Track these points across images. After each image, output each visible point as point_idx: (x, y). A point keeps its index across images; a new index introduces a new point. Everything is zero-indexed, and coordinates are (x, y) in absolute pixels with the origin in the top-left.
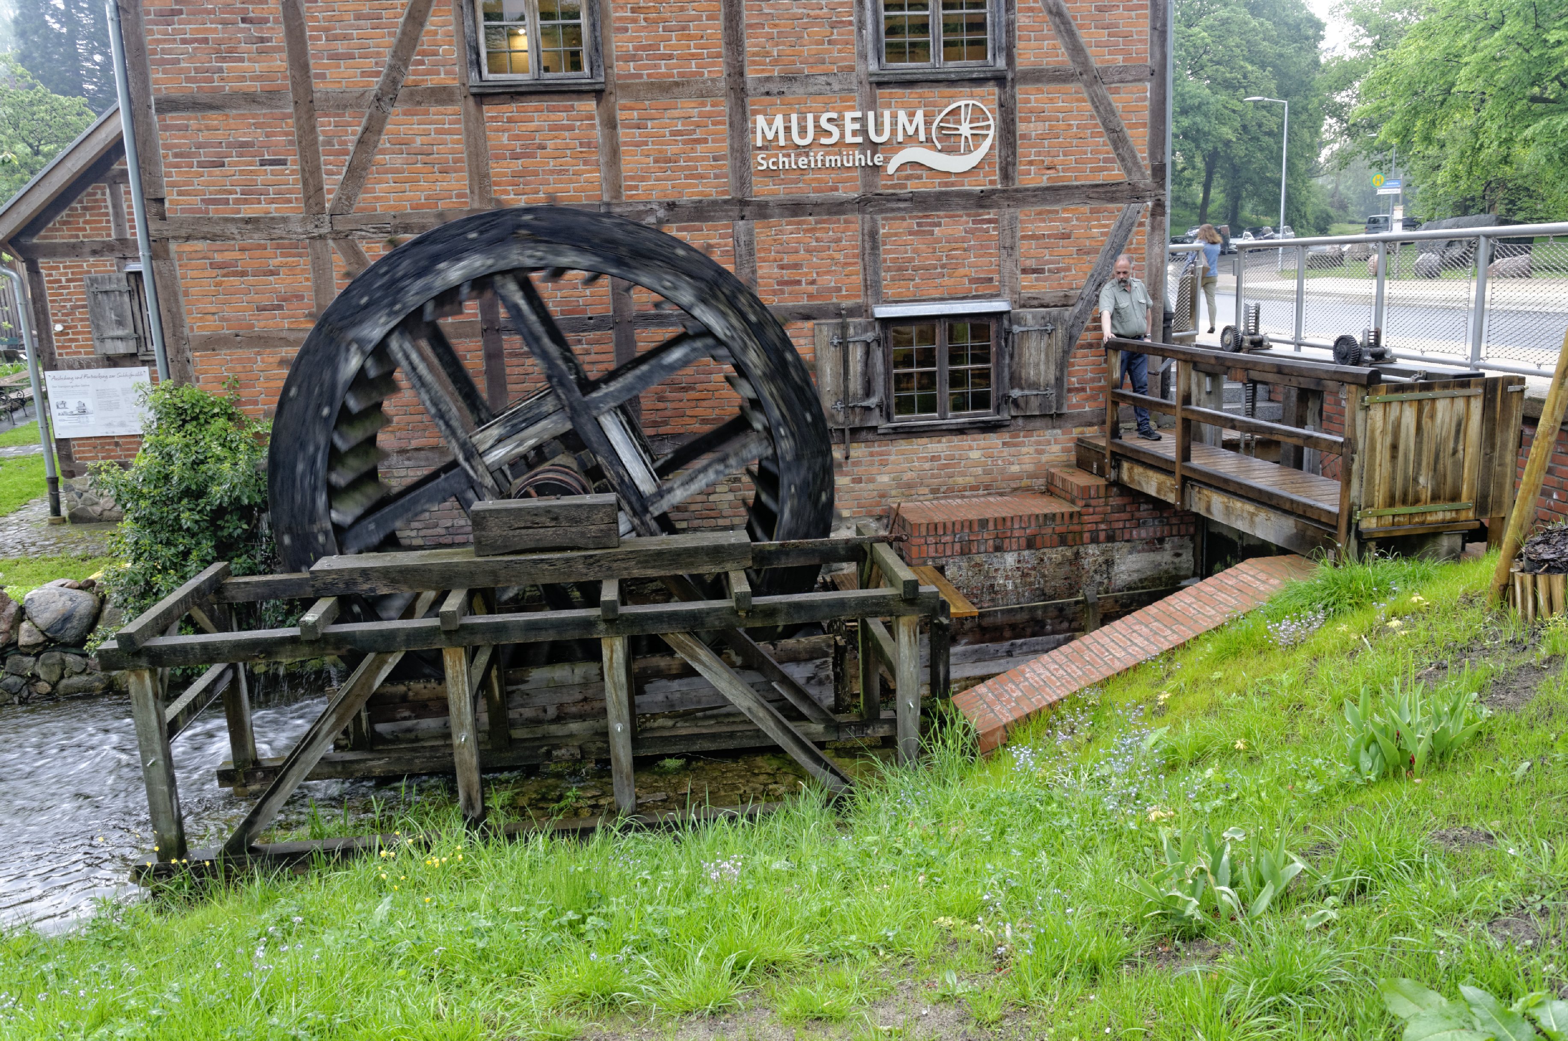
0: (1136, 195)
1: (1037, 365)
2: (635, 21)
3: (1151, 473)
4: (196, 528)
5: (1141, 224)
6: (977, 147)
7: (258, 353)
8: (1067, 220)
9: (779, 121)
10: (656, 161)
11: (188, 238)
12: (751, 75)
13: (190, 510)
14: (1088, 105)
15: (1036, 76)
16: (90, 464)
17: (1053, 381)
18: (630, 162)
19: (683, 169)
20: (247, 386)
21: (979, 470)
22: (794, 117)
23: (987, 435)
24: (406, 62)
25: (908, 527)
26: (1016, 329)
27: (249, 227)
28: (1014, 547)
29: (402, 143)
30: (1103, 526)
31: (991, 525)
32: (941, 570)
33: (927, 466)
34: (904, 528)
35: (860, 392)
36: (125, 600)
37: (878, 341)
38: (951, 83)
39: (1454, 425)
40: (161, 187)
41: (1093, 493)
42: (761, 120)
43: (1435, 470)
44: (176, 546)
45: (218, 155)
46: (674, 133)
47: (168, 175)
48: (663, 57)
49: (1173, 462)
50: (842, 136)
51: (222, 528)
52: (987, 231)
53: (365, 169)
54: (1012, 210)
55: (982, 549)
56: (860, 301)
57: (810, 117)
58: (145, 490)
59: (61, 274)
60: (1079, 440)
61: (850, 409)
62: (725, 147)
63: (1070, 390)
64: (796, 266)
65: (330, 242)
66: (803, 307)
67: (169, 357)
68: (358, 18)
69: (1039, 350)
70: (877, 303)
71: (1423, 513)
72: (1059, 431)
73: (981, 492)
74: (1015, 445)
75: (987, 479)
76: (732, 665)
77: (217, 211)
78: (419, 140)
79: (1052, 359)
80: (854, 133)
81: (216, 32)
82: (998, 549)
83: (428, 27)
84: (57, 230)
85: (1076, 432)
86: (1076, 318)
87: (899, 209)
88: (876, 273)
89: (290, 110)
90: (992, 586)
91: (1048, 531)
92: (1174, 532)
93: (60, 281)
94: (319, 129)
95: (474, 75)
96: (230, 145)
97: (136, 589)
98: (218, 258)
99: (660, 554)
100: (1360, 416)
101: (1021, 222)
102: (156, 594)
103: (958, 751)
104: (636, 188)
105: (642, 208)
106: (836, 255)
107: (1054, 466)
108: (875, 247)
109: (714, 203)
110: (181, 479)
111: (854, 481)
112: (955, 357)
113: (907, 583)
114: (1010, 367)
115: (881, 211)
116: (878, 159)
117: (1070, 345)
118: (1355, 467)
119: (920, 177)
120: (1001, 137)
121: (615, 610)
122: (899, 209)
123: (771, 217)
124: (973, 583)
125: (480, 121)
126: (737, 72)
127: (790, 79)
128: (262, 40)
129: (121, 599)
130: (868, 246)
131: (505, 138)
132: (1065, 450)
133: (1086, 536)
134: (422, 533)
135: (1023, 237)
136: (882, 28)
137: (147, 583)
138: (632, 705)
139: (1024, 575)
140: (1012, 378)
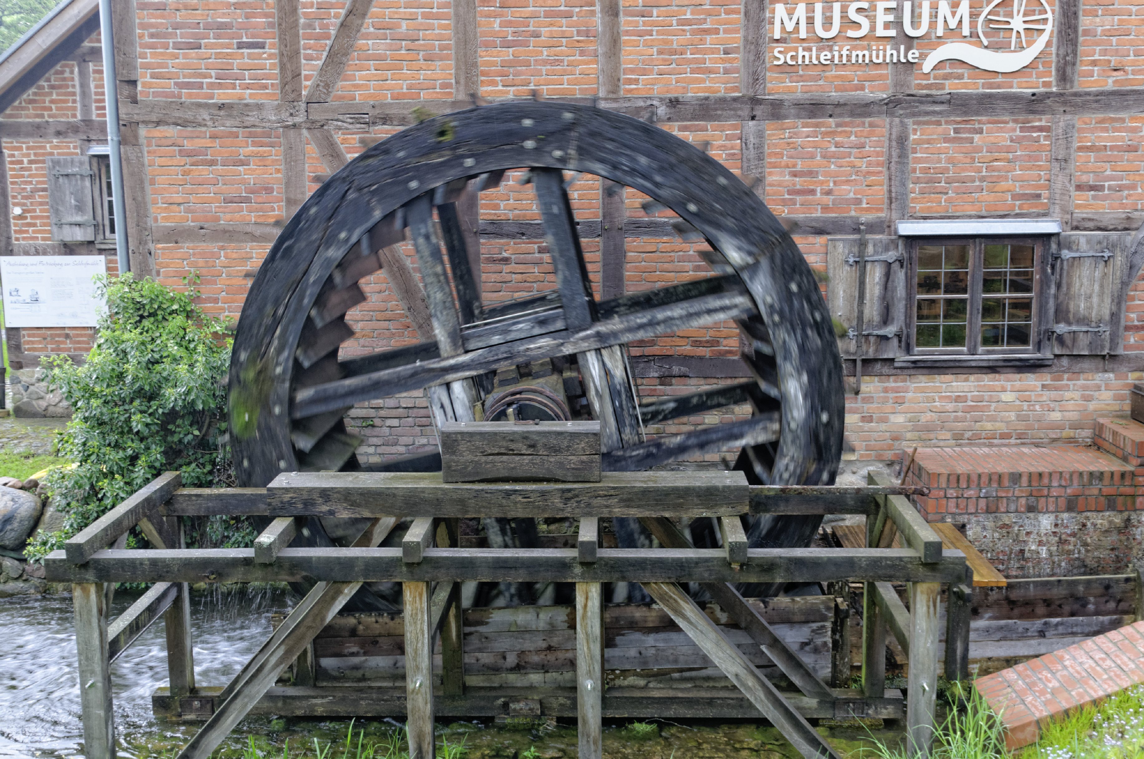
4: (146, 432)
6: (1030, 43)
7: (222, 248)
8: (1134, 130)
9: (801, 11)
10: (660, 52)
11: (158, 123)
13: (141, 412)
16: (43, 359)
17: (1107, 317)
19: (689, 61)
20: (208, 282)
21: (1012, 416)
22: (819, 7)
23: (1023, 376)
25: (924, 476)
26: (1066, 254)
27: (222, 113)
28: (1051, 508)
31: (1024, 481)
32: (962, 528)
33: (950, 406)
34: (919, 477)
35: (877, 318)
36: (68, 504)
37: (901, 262)
40: (135, 68)
42: (780, 10)
44: (124, 449)
45: (195, 36)
46: (681, 23)
47: (144, 56)
50: (873, 28)
51: (173, 433)
52: (1037, 140)
53: (346, 54)
54: (1068, 117)
55: (1013, 507)
56: (882, 215)
57: (837, 7)
58: (97, 389)
59: (24, 155)
60: (1136, 387)
63: (1127, 328)
64: (811, 173)
65: (305, 132)
66: (816, 219)
67: (131, 248)
69: (1092, 280)
70: (902, 217)
72: (1112, 375)
73: (1013, 441)
74: (1056, 389)
75: (1021, 426)
76: (717, 622)
77: (190, 95)
78: (404, 24)
79: (1108, 291)
80: (887, 25)
82: (1031, 509)
84: (23, 109)
85: (1132, 378)
87: (934, 113)
88: (904, 185)
90: (1022, 551)
93: (21, 162)
94: (301, 11)
97: (80, 493)
98: (188, 145)
99: (645, 492)
101: (1080, 130)
102: (100, 500)
103: (980, 746)
104: (636, 81)
105: (641, 104)
106: (857, 162)
107: (1103, 416)
108: (903, 155)
109: (723, 100)
110: (136, 379)
111: (863, 419)
113: (928, 545)
114: (1056, 297)
115: (914, 115)
117: (1130, 275)
119: (960, 77)
120: (1060, 32)
121: (593, 552)
122: (934, 113)
123: (786, 117)
124: (1000, 546)
129: (64, 502)
130: (895, 154)
131: (496, 27)
134: (380, 450)
135: (1080, 149)
137: (92, 487)
138: (604, 660)
139: (1061, 542)
140: (1056, 311)
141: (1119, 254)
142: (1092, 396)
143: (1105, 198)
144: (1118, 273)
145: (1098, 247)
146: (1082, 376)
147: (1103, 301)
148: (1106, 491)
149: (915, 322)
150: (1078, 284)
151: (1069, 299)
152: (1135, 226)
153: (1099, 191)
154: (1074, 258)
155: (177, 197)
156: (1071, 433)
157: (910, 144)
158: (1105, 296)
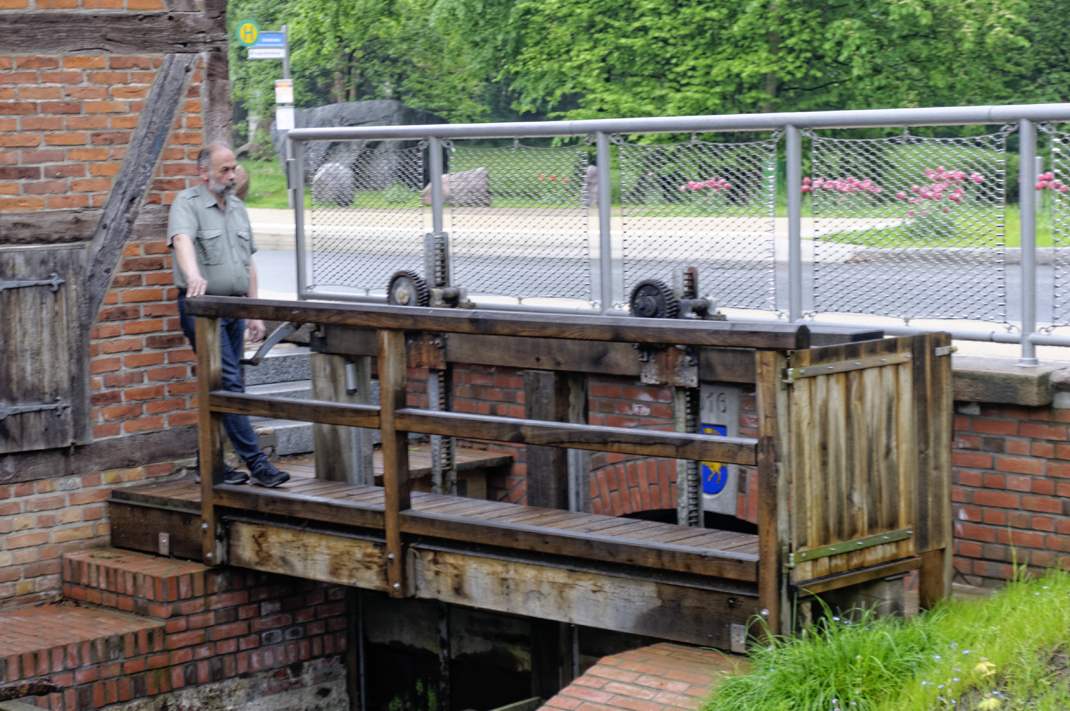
1: (37, 353)
3: (311, 540)
5: (193, 92)
8: (72, 79)
17: (65, 385)
30: (204, 652)
39: (884, 408)
41: (184, 589)
43: (869, 480)
49: (382, 513)
60: (115, 493)
63: (96, 400)
69: (39, 324)
71: (861, 550)
72: (77, 480)
79: (62, 341)
86: (97, 262)
91: (115, 670)
92: (316, 651)
100: (782, 398)
117: (90, 315)
118: (781, 483)
132: (91, 517)
133: (177, 674)
141: (73, 279)
142: (53, 517)
144: (74, 311)
145: (42, 270)
146: (36, 486)
147: (57, 359)
148: (131, 666)
150: (19, 333)
151: (10, 359)
152: (87, 233)
153: (29, 177)
154: (10, 290)
156: (25, 585)
158: (60, 349)
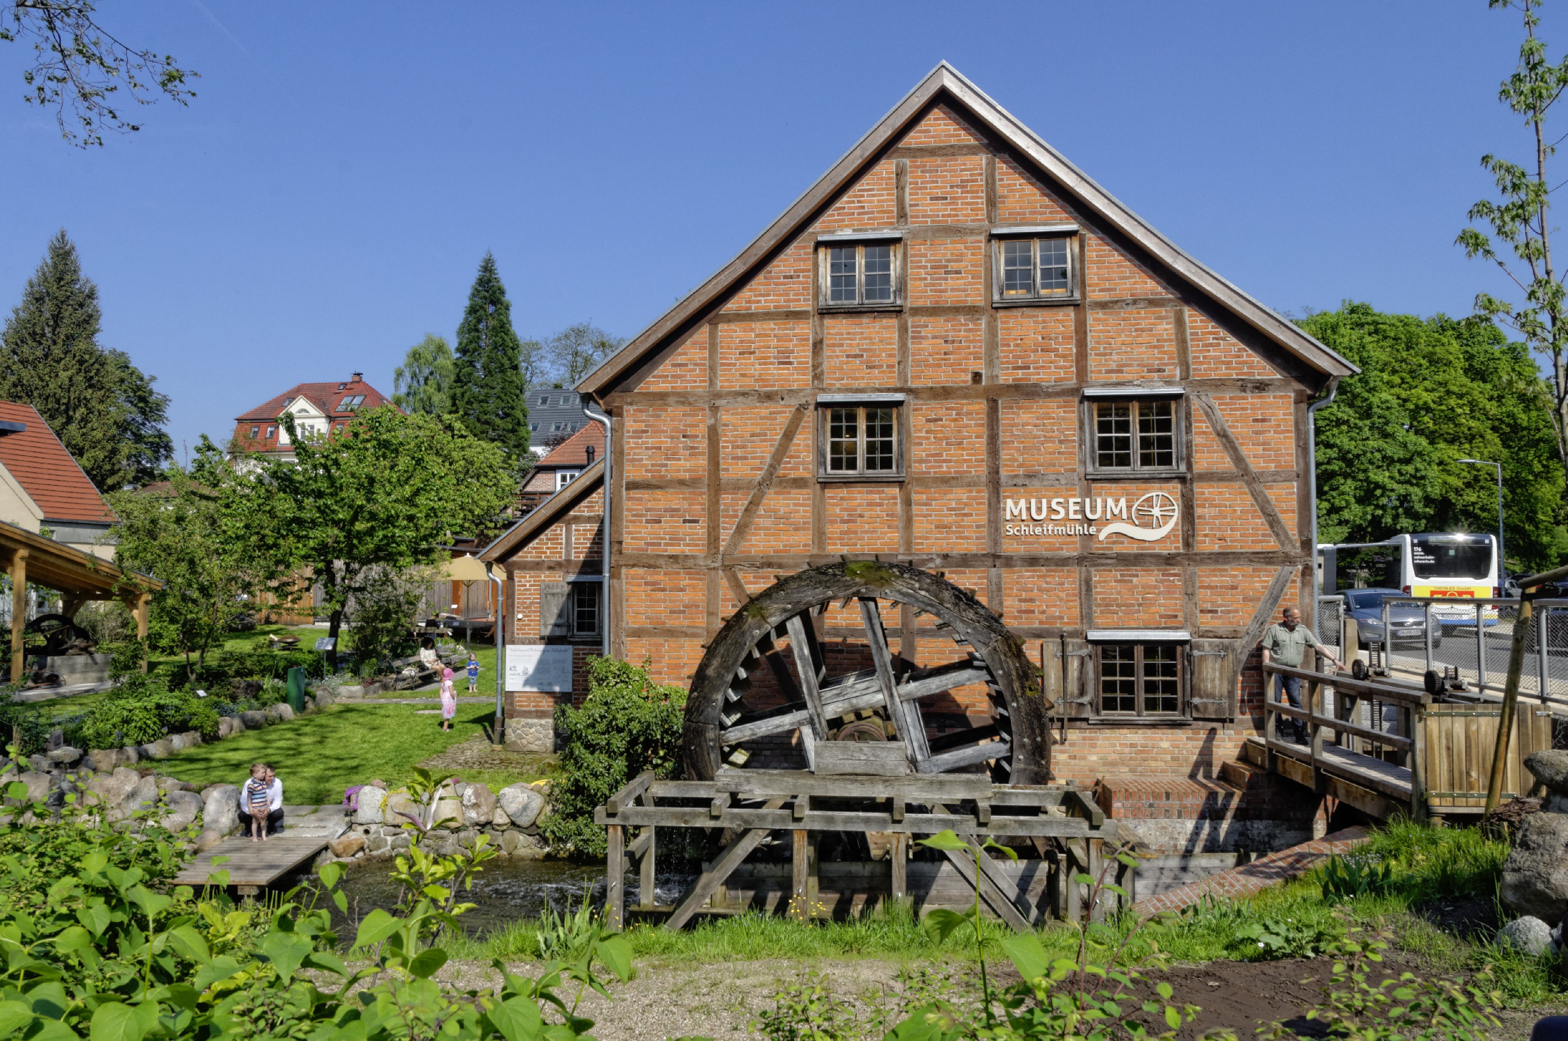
0: (1288, 560)
1: (1213, 680)
2: (927, 438)
5: (1294, 581)
6: (1165, 523)
8: (1234, 576)
9: (1022, 503)
11: (634, 566)
12: (1004, 473)
14: (1249, 497)
15: (1209, 477)
17: (1226, 693)
18: (920, 527)
21: (1169, 757)
22: (1033, 501)
24: (779, 462)
26: (1196, 653)
29: (773, 513)
33: (1127, 750)
35: (1076, 692)
38: (1146, 480)
42: (1010, 503)
46: (950, 509)
48: (945, 461)
50: (1067, 514)
56: (1078, 627)
57: (1044, 501)
61: (1067, 703)
62: (984, 520)
64: (1032, 600)
68: (752, 435)
69: (1214, 669)
80: (1076, 512)
81: (666, 442)
83: (795, 441)
88: (1090, 608)
89: (705, 490)
95: (822, 471)
96: (666, 510)
108: (1089, 589)
109: (976, 555)
111: (1070, 757)
112: (1150, 670)
116: (1092, 530)
120: (1183, 518)
125: (823, 499)
126: (994, 471)
127: (1030, 476)
128: (692, 448)
131: (838, 511)
136: (1096, 444)
143: (1219, 618)
149: (1101, 695)
155: (642, 610)
157: (1093, 583)
